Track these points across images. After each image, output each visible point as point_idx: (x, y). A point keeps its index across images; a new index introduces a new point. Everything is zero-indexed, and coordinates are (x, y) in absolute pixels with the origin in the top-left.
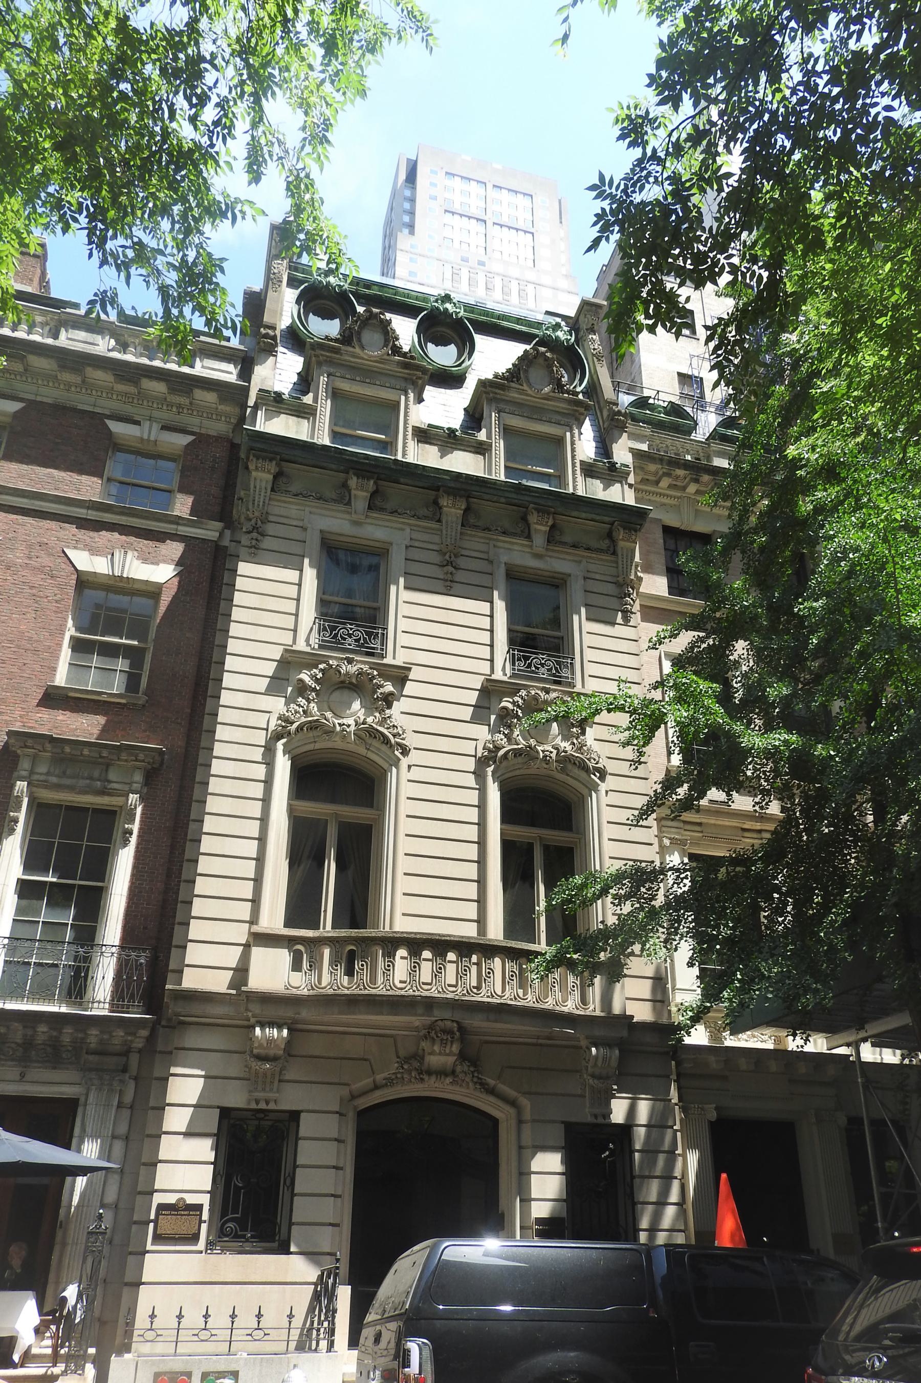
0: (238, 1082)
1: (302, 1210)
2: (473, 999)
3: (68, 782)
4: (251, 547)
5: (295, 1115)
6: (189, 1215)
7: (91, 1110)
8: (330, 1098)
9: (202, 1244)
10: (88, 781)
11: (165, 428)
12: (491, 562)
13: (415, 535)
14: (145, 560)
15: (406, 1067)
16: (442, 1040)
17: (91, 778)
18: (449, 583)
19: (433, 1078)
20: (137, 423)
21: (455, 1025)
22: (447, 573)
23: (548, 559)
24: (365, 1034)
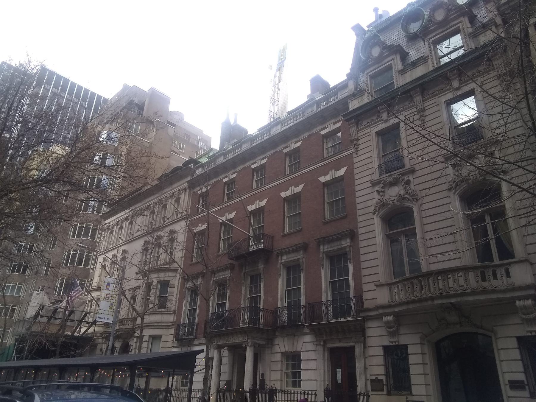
0: (386, 337)
1: (414, 380)
3: (332, 249)
4: (355, 152)
5: (406, 346)
8: (416, 339)
9: (385, 392)
10: (337, 247)
11: (334, 124)
12: (438, 105)
13: (407, 113)
17: (338, 246)
18: (423, 124)
20: (327, 128)
22: (421, 121)
23: (463, 88)
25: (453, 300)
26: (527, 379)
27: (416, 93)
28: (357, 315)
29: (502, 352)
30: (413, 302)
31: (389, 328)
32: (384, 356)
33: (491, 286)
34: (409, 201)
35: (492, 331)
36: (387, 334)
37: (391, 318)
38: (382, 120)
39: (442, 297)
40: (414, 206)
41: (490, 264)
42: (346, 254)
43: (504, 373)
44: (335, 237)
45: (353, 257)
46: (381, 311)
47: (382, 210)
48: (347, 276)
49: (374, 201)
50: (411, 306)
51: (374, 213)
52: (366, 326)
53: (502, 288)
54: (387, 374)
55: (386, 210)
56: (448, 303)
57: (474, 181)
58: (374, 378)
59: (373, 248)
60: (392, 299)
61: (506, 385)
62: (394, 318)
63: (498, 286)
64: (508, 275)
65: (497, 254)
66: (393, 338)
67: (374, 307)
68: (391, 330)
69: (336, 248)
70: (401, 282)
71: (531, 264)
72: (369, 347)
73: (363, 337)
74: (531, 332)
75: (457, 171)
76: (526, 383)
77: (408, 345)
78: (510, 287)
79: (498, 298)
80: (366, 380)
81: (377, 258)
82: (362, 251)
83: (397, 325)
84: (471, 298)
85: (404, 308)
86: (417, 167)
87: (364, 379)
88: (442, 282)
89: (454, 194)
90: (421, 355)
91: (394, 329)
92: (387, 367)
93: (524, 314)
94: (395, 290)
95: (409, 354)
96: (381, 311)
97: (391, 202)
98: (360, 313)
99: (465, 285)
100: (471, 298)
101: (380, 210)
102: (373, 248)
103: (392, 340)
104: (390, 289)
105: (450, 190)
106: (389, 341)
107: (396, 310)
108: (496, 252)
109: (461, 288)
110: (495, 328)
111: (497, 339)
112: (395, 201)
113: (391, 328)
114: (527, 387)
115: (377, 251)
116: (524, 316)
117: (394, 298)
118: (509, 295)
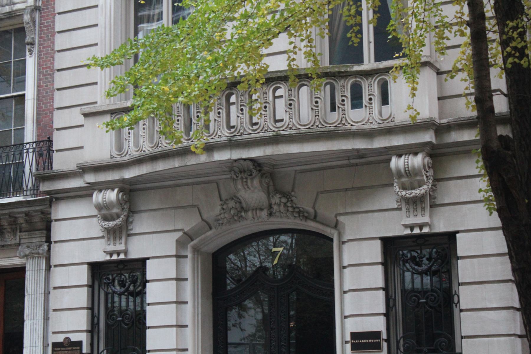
0: (98, 241)
2: (252, 136)
6: (73, 350)
15: (225, 207)
16: (242, 178)
19: (250, 214)
21: (250, 163)
24: (193, 184)
25: (256, 153)
26: (388, 329)
28: (36, 188)
29: (347, 271)
30: (165, 156)
31: (106, 218)
32: (91, 286)
33: (343, 122)
35: (336, 226)
36: (101, 235)
37: (112, 195)
41: (349, 70)
42: (21, 31)
43: (346, 317)
45: (40, 38)
46: (90, 178)
48: (21, 91)
50: (161, 166)
52: (53, 217)
53: (365, 127)
54: (93, 330)
56: (245, 160)
58: (60, 338)
59: (86, 18)
60: (120, 148)
61: (347, 342)
62: (121, 194)
63: (357, 122)
64: (385, 100)
65: (372, 45)
66: (115, 244)
67: (76, 168)
68: (111, 224)
71: (439, 73)
72: (56, 266)
73: (46, 242)
74: (412, 228)
76: (384, 336)
77: (148, 258)
78: (382, 125)
79: (358, 150)
80: (45, 346)
81: (96, 44)
82: (61, 23)
83: (125, 214)
84: (294, 149)
87: (40, 344)
88: (237, 108)
90: (174, 282)
91: (118, 222)
92: (96, 311)
93: (404, 188)
95: (148, 281)
96: (90, 178)
98: (41, 185)
99: (286, 118)
100: (294, 149)
102: (86, 18)
103: (112, 248)
106: (105, 252)
107: (129, 174)
108: (372, 39)
109: (279, 124)
110: (341, 219)
111: (343, 243)
113: (113, 219)
114: (385, 345)
115: (96, 25)
116: (404, 193)
117: (126, 147)
118: (379, 143)
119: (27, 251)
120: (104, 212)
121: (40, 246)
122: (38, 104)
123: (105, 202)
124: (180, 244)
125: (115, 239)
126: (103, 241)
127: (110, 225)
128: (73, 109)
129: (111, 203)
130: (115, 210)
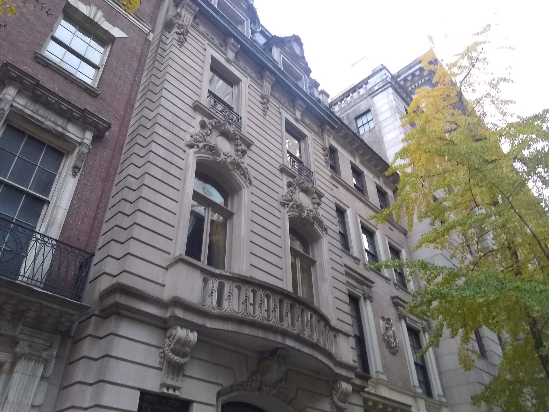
7: (16, 376)
14: (108, 20)
27: (269, 78)
31: (173, 351)
34: (242, 176)
37: (193, 337)
38: (226, 55)
39: (298, 338)
40: (245, 187)
44: (64, 106)
46: (179, 313)
47: (205, 153)
49: (191, 131)
50: (246, 330)
51: (191, 146)
55: (208, 158)
57: (307, 217)
66: (172, 379)
69: (48, 123)
70: (231, 280)
75: (292, 192)
81: (175, 214)
85: (230, 327)
86: (253, 148)
89: (287, 212)
94: (213, 287)
96: (179, 313)
97: (223, 156)
101: (203, 150)
103: (169, 382)
104: (205, 281)
105: (283, 205)
112: (229, 160)
119: (27, 351)
120: (178, 347)
121: (45, 350)
122: (67, 217)
123: (187, 339)
124: (219, 394)
125: (173, 374)
126: (158, 372)
127: (181, 361)
128: (149, 247)
129: (190, 341)
130: (187, 349)
